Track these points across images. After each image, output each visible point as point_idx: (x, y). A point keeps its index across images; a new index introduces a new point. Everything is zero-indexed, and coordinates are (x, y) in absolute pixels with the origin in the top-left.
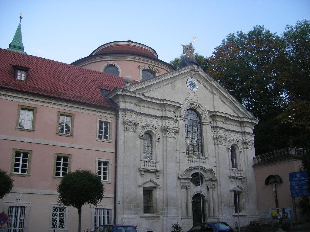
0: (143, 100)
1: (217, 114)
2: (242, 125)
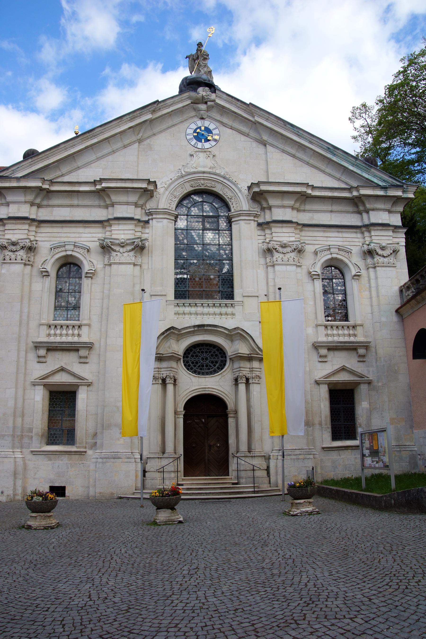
0: (49, 192)
2: (361, 208)
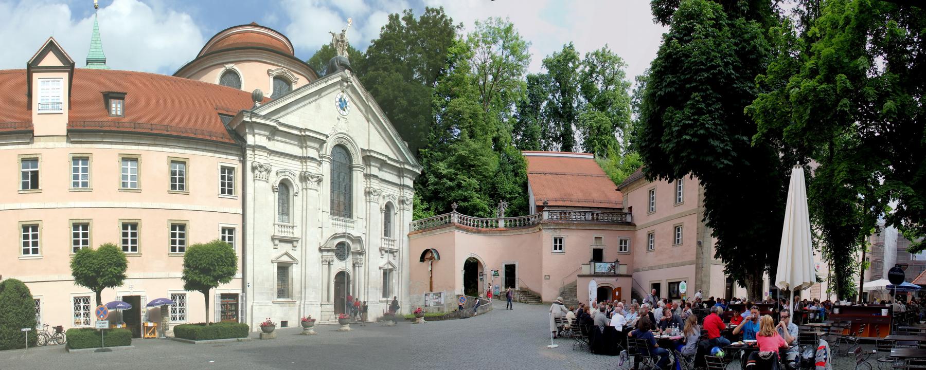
1: (372, 154)
